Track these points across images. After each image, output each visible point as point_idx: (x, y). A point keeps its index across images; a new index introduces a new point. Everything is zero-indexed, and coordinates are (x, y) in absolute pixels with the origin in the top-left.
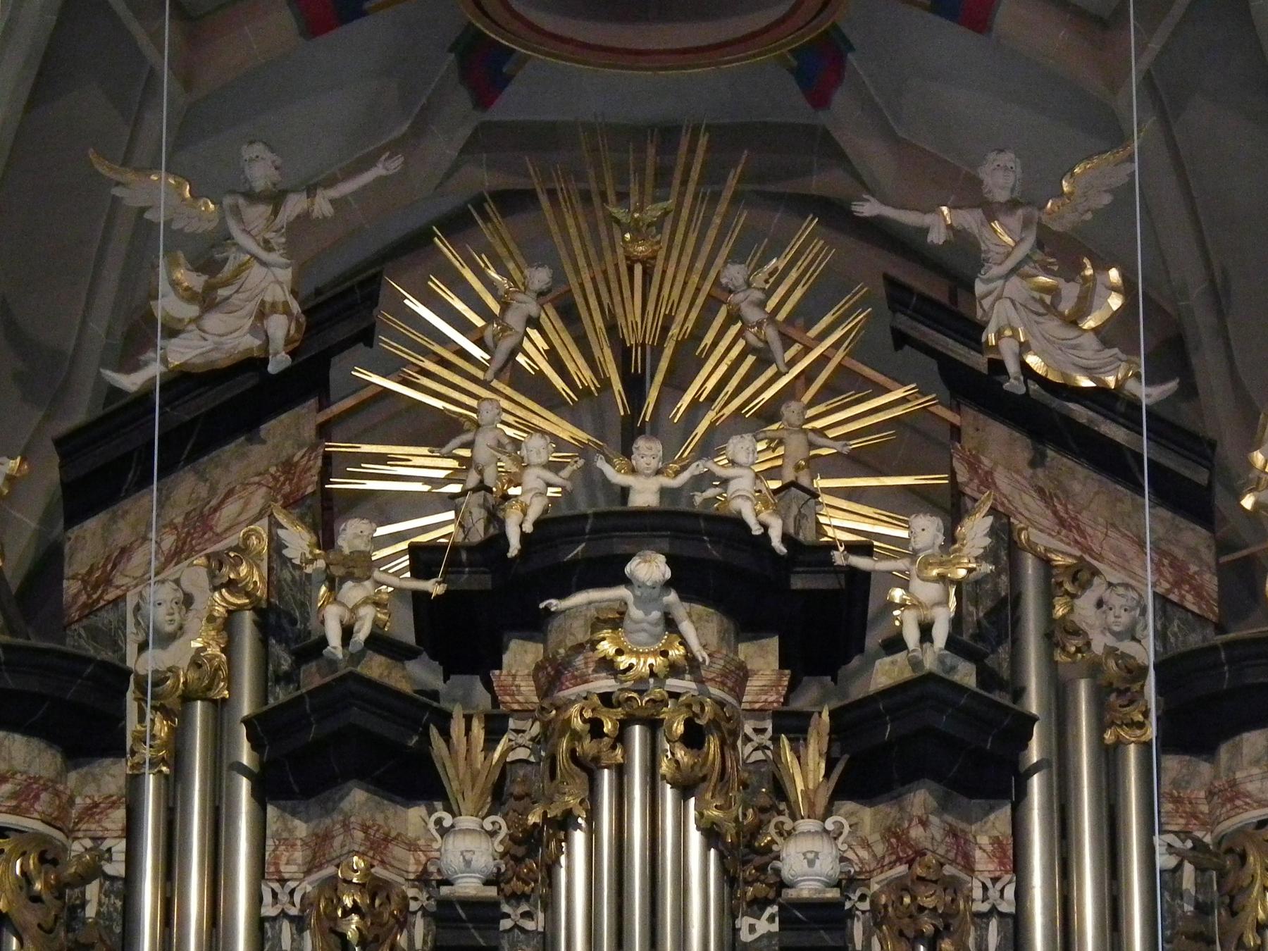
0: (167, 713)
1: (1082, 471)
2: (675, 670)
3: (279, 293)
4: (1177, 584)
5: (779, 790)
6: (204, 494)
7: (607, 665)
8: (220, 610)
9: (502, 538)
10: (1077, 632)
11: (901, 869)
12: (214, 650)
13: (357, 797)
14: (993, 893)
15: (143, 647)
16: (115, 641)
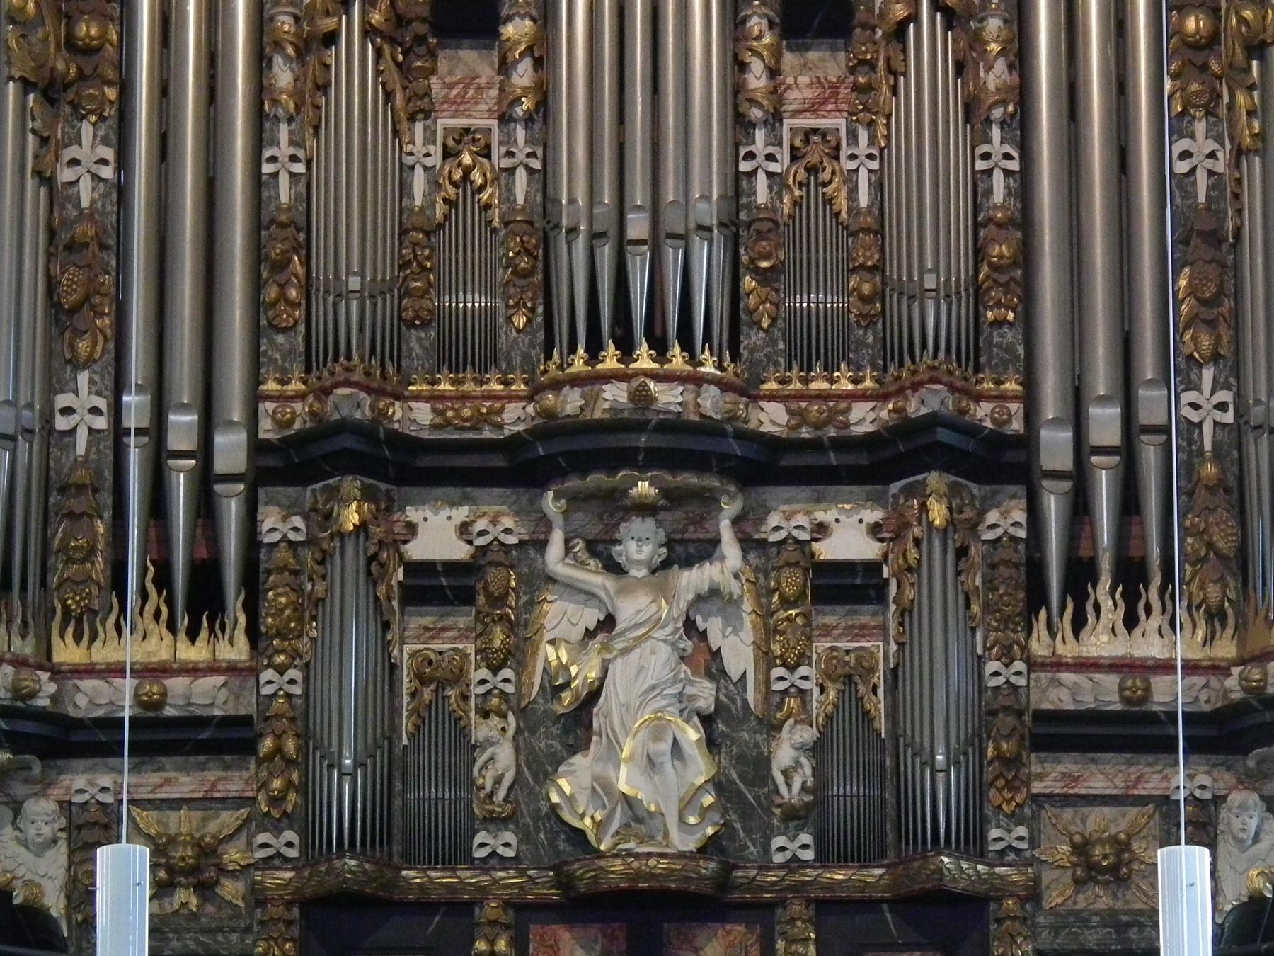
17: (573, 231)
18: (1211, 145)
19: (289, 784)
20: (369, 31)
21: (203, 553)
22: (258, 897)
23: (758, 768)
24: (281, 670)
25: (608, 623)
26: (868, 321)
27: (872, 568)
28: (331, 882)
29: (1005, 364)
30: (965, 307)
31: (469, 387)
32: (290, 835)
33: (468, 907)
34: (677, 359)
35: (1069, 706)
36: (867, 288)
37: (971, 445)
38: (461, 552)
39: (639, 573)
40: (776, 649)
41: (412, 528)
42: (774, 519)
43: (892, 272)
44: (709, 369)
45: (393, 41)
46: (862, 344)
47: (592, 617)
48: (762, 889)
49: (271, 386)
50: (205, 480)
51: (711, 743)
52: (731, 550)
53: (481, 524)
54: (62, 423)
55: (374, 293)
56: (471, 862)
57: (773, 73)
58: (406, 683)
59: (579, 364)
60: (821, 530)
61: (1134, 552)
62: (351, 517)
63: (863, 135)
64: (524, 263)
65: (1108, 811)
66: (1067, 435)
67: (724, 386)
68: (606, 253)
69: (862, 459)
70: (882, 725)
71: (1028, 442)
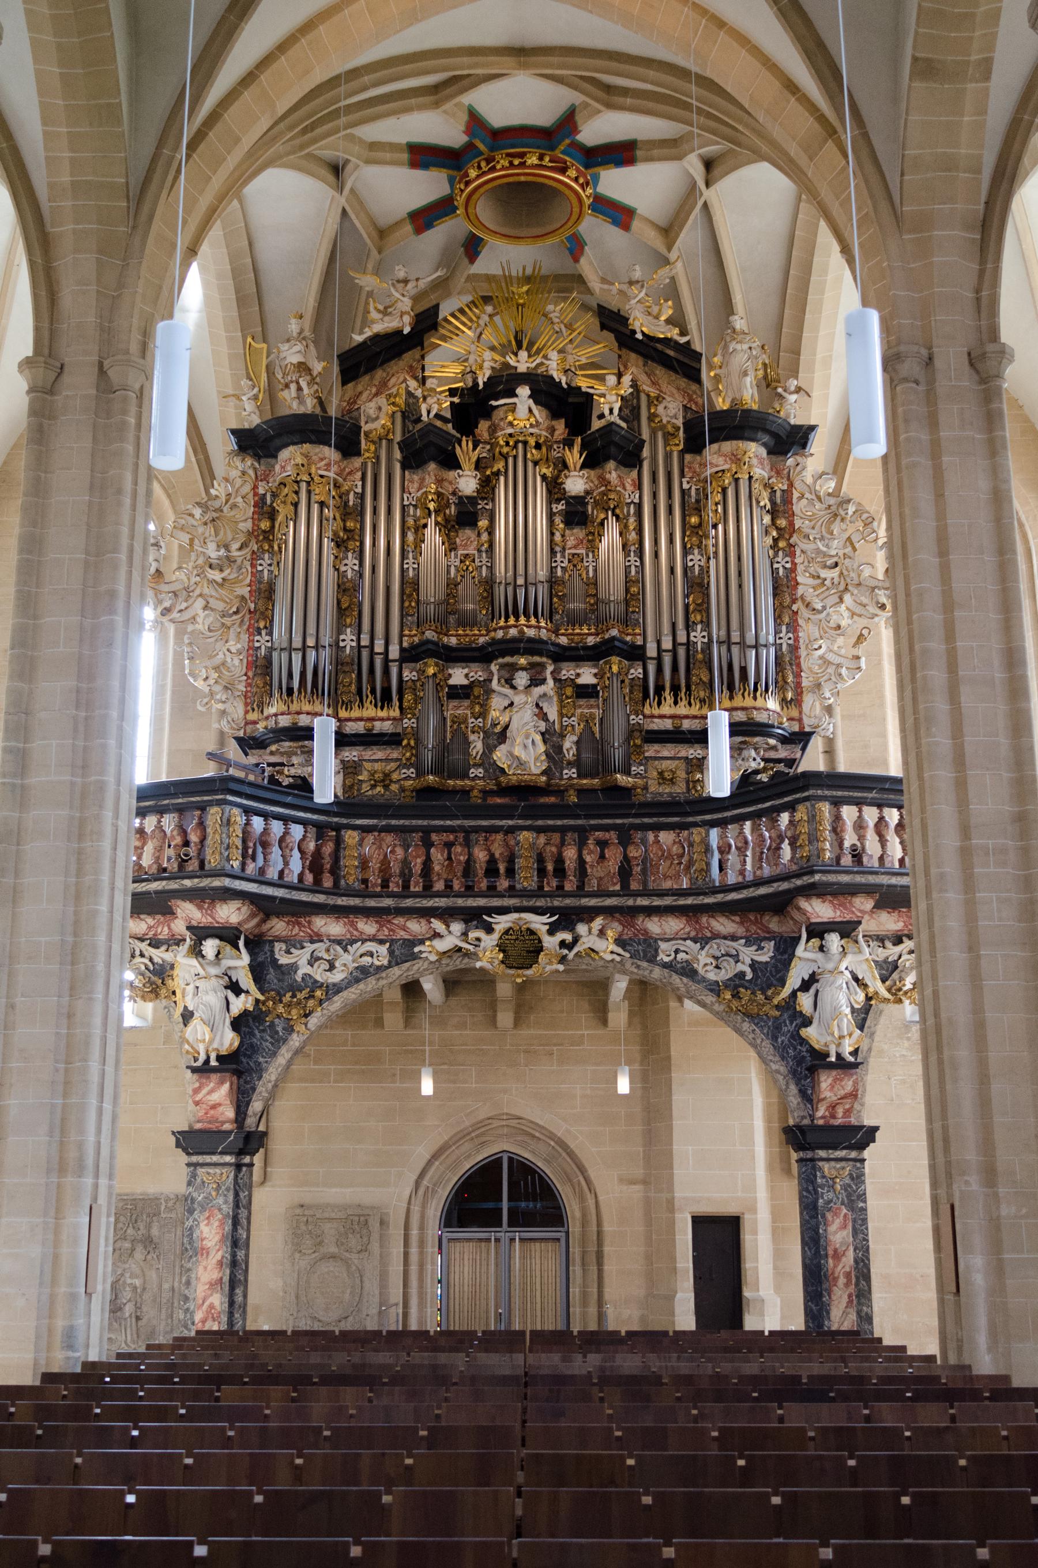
0: (373, 442)
1: (659, 368)
2: (531, 426)
3: (408, 309)
4: (689, 402)
5: (565, 466)
6: (385, 375)
7: (511, 424)
8: (390, 412)
9: (476, 384)
10: (657, 416)
11: (603, 488)
12: (389, 424)
13: (432, 466)
14: (632, 496)
15: (366, 423)
16: (358, 419)
17: (500, 583)
18: (699, 557)
19: (412, 754)
20: (437, 523)
21: (386, 685)
22: (403, 789)
23: (559, 749)
24: (410, 719)
25: (512, 704)
26: (593, 611)
27: (594, 686)
28: (425, 784)
29: (635, 625)
30: (623, 607)
31: (468, 632)
32: (412, 770)
33: (468, 792)
34: (533, 621)
35: (656, 728)
36: (592, 601)
37: (625, 647)
38: (465, 682)
39: (521, 688)
40: (564, 712)
41: (450, 675)
42: (564, 672)
43: (600, 596)
44: (543, 624)
45: (445, 527)
46: (591, 618)
47: (506, 703)
48: (560, 786)
49: (406, 632)
50: (386, 661)
51: (545, 741)
52: (550, 682)
53: (472, 674)
54: (342, 644)
55: (438, 604)
56: (469, 778)
57: (563, 536)
58: (449, 724)
59: (502, 623)
60: (578, 675)
61: (676, 683)
62: (431, 671)
63: (591, 555)
64: (485, 594)
65: (669, 762)
66: (655, 645)
67: (548, 630)
68: (510, 589)
69: (591, 653)
70: (598, 736)
71: (643, 648)
